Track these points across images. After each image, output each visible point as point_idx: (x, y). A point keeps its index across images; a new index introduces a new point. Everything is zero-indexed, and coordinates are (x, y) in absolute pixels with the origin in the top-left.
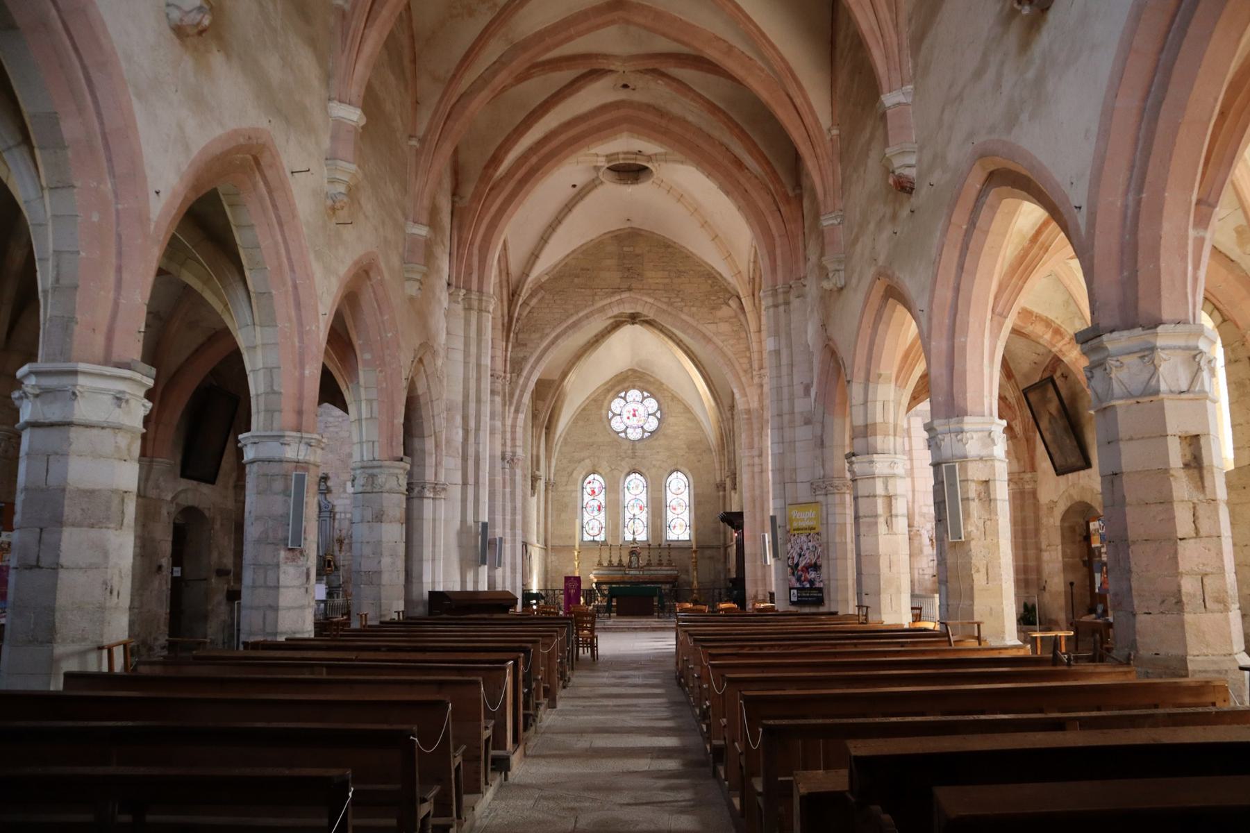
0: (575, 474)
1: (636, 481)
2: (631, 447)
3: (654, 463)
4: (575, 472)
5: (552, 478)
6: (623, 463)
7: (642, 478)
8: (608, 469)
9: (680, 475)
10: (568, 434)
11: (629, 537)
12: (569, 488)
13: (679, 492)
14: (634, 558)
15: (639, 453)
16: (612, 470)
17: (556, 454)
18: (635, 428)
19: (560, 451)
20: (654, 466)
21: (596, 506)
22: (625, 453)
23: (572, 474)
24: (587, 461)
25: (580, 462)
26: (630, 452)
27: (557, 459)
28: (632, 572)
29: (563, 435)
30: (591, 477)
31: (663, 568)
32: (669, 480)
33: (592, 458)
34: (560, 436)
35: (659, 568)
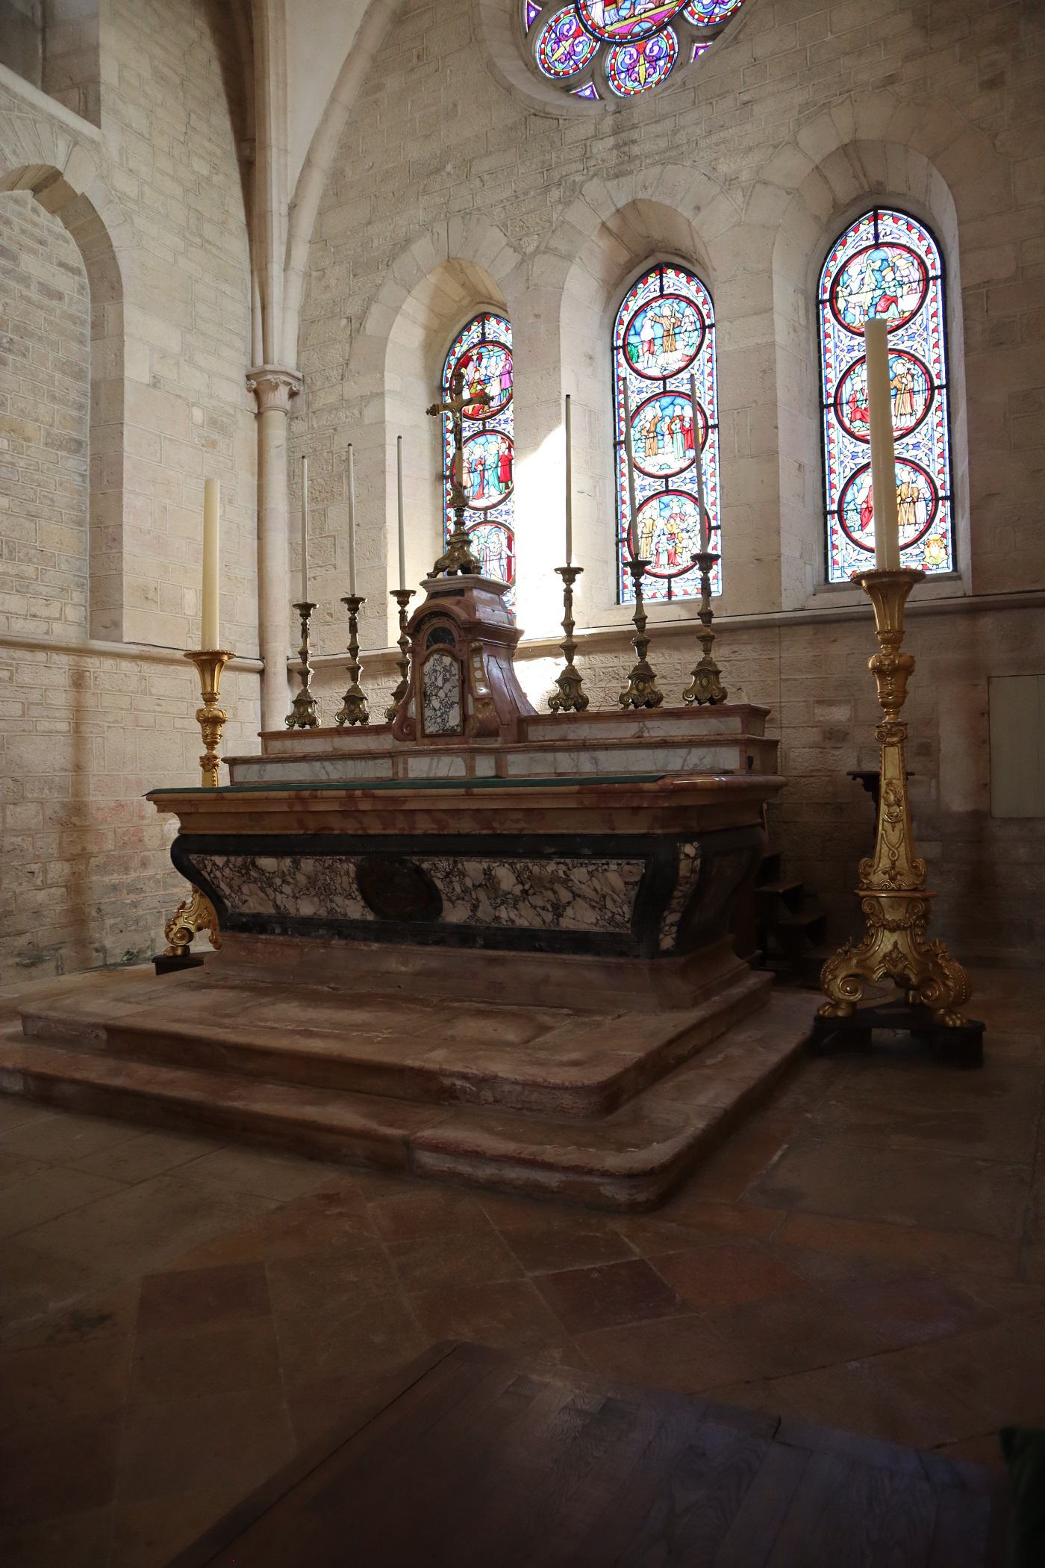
0: (371, 325)
1: (666, 308)
2: (609, 121)
3: (724, 168)
4: (375, 309)
5: (285, 353)
6: (576, 214)
7: (690, 289)
8: (511, 258)
9: (892, 227)
10: (346, 148)
11: (700, 596)
12: (352, 389)
13: (892, 315)
14: (439, 666)
15: (648, 141)
16: (525, 259)
17: (301, 253)
18: (647, 35)
19: (320, 240)
20: (730, 182)
21: (491, 460)
22: (586, 157)
23: (362, 318)
24: (422, 250)
25: (390, 258)
26: (602, 148)
27: (307, 275)
28: (419, 768)
29: (325, 157)
30: (474, 334)
31: (658, 729)
32: (833, 267)
33: (440, 228)
34: (308, 163)
35: (628, 730)
